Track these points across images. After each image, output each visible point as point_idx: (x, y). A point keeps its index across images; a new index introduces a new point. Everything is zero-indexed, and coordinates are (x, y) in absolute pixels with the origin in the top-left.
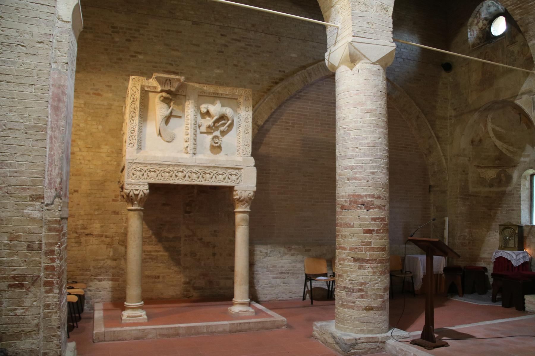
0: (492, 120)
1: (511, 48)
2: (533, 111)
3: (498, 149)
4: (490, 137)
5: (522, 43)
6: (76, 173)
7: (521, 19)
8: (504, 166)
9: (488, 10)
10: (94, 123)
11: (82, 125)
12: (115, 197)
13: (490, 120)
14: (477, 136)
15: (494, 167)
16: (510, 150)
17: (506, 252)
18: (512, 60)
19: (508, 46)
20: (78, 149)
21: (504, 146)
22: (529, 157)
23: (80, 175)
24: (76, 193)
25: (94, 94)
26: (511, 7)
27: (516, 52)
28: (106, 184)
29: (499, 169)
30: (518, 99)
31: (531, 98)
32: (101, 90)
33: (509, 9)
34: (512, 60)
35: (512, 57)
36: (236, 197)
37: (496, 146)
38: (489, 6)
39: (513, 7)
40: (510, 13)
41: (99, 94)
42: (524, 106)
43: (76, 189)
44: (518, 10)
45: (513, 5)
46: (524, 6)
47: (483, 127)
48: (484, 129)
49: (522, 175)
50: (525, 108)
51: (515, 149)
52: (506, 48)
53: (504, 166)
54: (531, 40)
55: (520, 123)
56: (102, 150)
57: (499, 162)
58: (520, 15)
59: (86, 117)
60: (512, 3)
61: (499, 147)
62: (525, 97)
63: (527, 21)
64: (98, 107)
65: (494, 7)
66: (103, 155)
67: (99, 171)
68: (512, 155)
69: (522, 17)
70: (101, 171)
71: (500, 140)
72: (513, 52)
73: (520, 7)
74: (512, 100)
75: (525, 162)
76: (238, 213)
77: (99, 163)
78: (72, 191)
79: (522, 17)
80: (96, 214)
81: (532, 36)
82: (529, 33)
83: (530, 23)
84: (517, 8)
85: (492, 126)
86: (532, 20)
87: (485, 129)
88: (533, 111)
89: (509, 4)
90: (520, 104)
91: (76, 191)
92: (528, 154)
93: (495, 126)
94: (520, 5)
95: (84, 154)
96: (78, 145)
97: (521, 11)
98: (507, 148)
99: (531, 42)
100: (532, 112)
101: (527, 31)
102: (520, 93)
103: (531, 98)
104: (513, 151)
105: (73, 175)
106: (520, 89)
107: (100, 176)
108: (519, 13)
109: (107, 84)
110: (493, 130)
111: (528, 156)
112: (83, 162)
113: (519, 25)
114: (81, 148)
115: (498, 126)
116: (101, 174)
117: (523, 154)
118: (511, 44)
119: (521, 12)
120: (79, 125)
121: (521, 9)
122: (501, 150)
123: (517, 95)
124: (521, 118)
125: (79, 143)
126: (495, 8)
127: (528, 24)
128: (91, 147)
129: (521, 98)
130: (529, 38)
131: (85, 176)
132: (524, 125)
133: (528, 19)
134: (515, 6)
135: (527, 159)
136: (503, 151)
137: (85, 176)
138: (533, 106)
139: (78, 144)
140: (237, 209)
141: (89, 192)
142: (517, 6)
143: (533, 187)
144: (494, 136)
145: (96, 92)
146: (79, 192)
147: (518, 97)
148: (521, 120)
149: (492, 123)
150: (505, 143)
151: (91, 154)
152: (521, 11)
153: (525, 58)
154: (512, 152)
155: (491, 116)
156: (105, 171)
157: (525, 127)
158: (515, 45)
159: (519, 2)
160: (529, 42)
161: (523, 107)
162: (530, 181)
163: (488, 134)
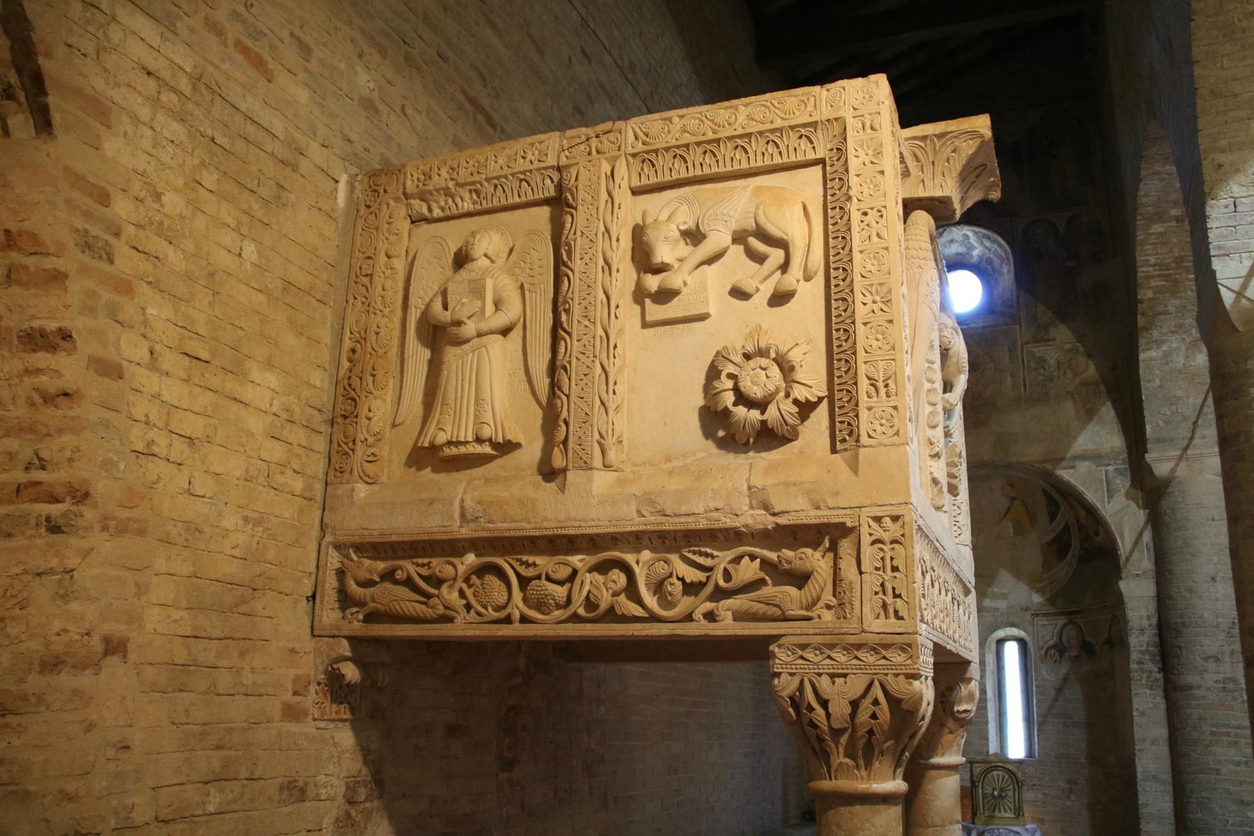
1: (1038, 350)
2: (1109, 502)
5: (1067, 346)
6: (124, 514)
7: (1150, 299)
9: (945, 247)
10: (227, 213)
11: (173, 202)
12: (295, 693)
17: (1011, 831)
18: (1041, 378)
19: (1028, 343)
20: (142, 354)
22: (1006, 599)
23: (142, 532)
24: (113, 660)
25: (239, 45)
26: (1151, 269)
27: (1052, 362)
28: (258, 606)
30: (1065, 468)
31: (1101, 470)
32: (273, 48)
33: (1143, 272)
34: (1041, 378)
35: (1042, 371)
36: (961, 708)
38: (952, 241)
39: (1155, 270)
40: (1140, 280)
41: (259, 64)
42: (1083, 485)
43: (116, 628)
44: (1159, 279)
45: (1158, 268)
46: (1177, 276)
49: (986, 640)
50: (1084, 491)
52: (1022, 346)
54: (1147, 349)
56: (248, 393)
58: (1155, 293)
59: (196, 161)
60: (1158, 261)
62: (1083, 466)
63: (1161, 308)
64: (250, 129)
65: (961, 245)
66: (256, 424)
67: (231, 521)
69: (1158, 296)
70: (241, 523)
72: (1041, 362)
73: (1169, 275)
74: (1048, 466)
75: (996, 610)
76: (943, 772)
77: (234, 466)
78: (96, 643)
79: (1158, 296)
80: (211, 809)
81: (1156, 341)
82: (1151, 334)
83: (1166, 313)
84: (1159, 276)
86: (1173, 308)
88: (1109, 502)
89: (1151, 263)
90: (1071, 480)
91: (115, 647)
92: (1003, 591)
94: (1171, 272)
95: (173, 391)
96: (145, 323)
97: (1163, 283)
99: (1148, 352)
100: (1104, 502)
101: (1150, 329)
102: (1069, 455)
103: (1101, 470)
105: (105, 528)
106: (1069, 447)
107: (236, 553)
108: (1157, 286)
109: (298, 32)
111: (1004, 596)
112: (161, 447)
113: (1139, 311)
114: (158, 348)
116: (241, 539)
117: (989, 590)
118: (1037, 342)
119: (1163, 286)
120: (158, 196)
121: (1166, 281)
123: (1062, 459)
124: (1009, 508)
125: (151, 311)
126: (961, 249)
127: (1160, 314)
128: (205, 355)
129: (1073, 467)
130: (1147, 343)
131: (167, 541)
132: (1010, 525)
133: (1166, 306)
134: (1160, 270)
135: (1002, 604)
137: (167, 541)
138: (1108, 490)
139: (143, 309)
140: (943, 755)
141: (181, 656)
142: (1164, 272)
143: (1003, 668)
145: (249, 43)
146: (133, 656)
147: (1064, 464)
148: (1006, 514)
151: (205, 399)
152: (1163, 283)
153: (1077, 380)
156: (258, 522)
158: (1047, 346)
159: (1174, 265)
160: (1144, 351)
161: (1081, 488)
162: (995, 655)
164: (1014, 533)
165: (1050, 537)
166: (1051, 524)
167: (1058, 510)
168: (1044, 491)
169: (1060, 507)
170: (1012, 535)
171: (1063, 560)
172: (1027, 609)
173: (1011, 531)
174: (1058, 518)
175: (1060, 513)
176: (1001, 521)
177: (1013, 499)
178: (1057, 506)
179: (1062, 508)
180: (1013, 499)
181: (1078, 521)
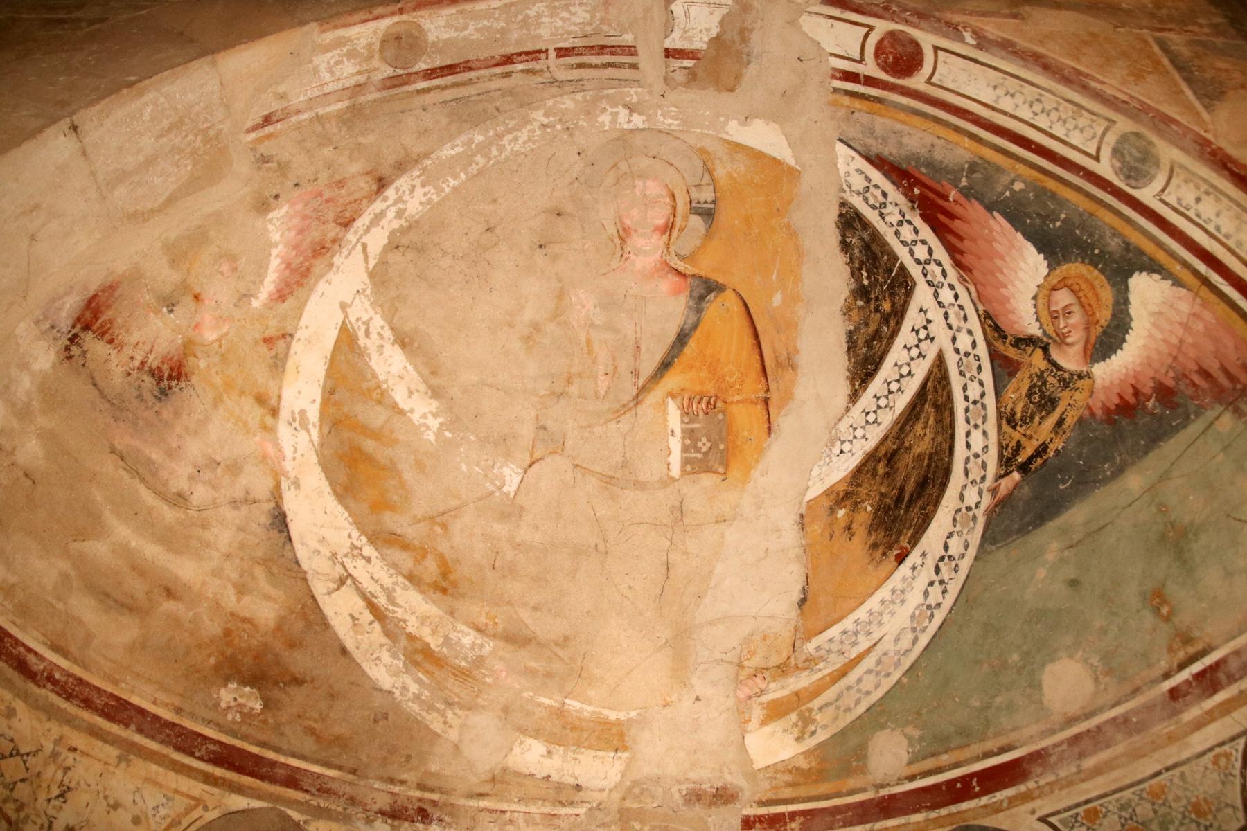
0: (394, 245)
3: (294, 572)
4: (275, 412)
8: (293, 780)
13: (377, 240)
14: (170, 303)
15: (186, 741)
16: (412, 627)
21: (358, 569)
29: (239, 790)
37: (280, 521)
47: (275, 263)
48: (269, 285)
51: (468, 638)
53: (293, 780)
55: (644, 390)
57: (258, 706)
61: (302, 553)
68: (414, 688)
71: (344, 492)
85: (362, 311)
87: (281, 295)
92: (612, 715)
93: (378, 322)
98: (382, 601)
104: (434, 643)
110: (347, 341)
115: (403, 341)
122: (319, 588)
124: (682, 339)
136: (328, 611)
144: (313, 414)
148: (665, 365)
149: (379, 277)
150: (383, 539)
154: (427, 652)
155: (414, 206)
157: (676, 444)
163: (278, 365)
164: (686, 462)
165: (841, 468)
166: (854, 397)
167: (898, 314)
168: (850, 221)
169: (909, 293)
170: (676, 471)
171: (901, 559)
172: (724, 796)
173: (676, 458)
174: (897, 354)
175: (912, 318)
176: (637, 399)
177: (706, 289)
178: (902, 285)
179: (922, 295)
180: (706, 289)
181: (994, 327)
